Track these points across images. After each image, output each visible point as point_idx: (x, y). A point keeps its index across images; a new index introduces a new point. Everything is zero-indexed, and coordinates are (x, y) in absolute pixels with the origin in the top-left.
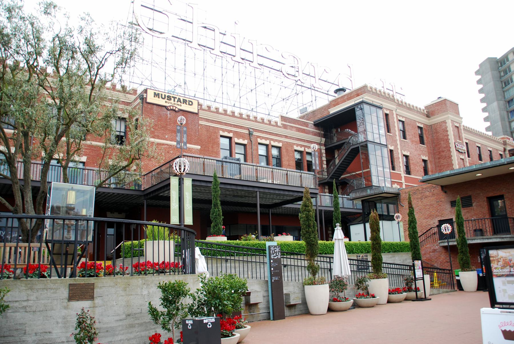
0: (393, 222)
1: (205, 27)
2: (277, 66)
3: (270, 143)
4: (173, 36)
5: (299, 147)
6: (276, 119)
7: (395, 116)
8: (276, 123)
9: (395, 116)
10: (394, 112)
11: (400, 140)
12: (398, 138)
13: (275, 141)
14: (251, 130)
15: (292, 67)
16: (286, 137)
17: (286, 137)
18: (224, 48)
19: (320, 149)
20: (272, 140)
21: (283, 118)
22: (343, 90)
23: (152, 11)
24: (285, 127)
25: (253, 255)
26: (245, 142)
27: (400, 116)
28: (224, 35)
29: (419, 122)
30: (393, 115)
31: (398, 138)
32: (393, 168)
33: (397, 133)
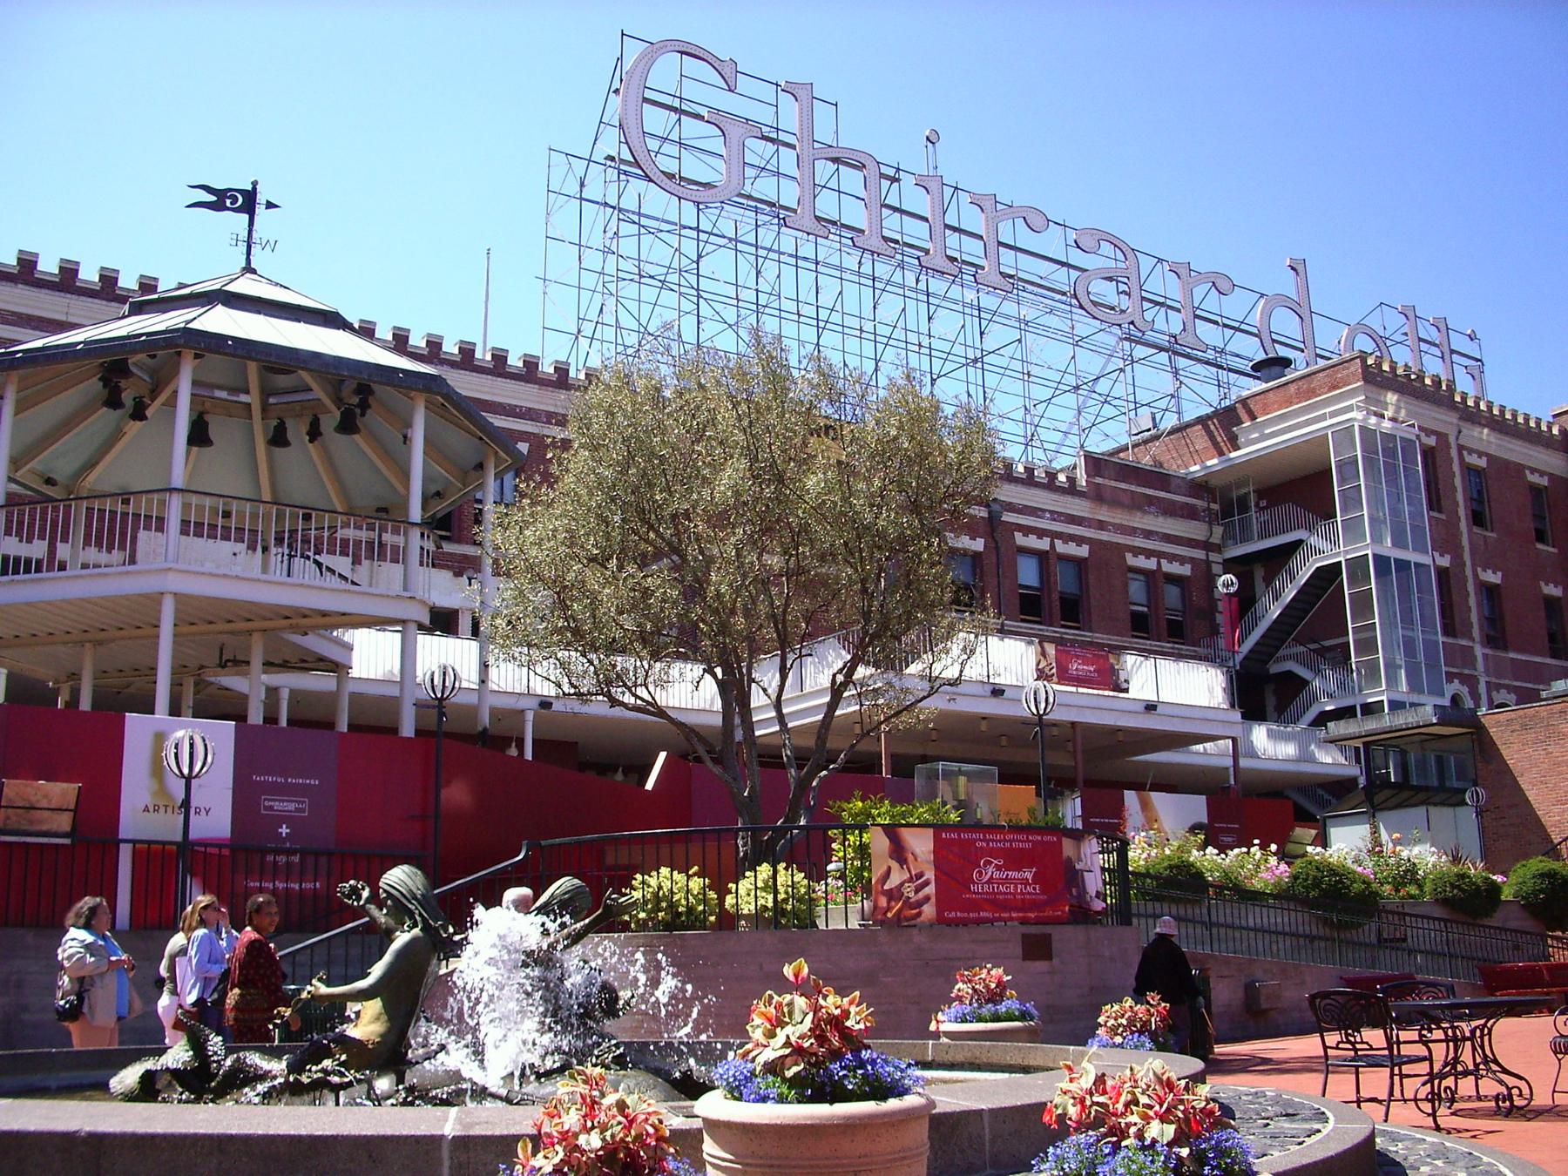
0: (1460, 810)
1: (835, 160)
2: (1061, 278)
3: (1052, 545)
4: (740, 195)
5: (1142, 557)
6: (1067, 460)
7: (1454, 452)
8: (1072, 480)
9: (1454, 452)
10: (1452, 439)
11: (1470, 532)
12: (1463, 525)
13: (1067, 538)
14: (996, 507)
15: (1110, 279)
16: (1101, 525)
17: (1101, 525)
18: (892, 223)
19: (1208, 563)
20: (1060, 535)
21: (1095, 463)
22: (1285, 363)
23: (674, 116)
24: (1097, 495)
25: (1189, 901)
26: (978, 545)
27: (1471, 451)
28: (894, 180)
29: (1533, 470)
30: (1448, 447)
31: (1463, 525)
32: (1449, 630)
33: (1462, 512)
